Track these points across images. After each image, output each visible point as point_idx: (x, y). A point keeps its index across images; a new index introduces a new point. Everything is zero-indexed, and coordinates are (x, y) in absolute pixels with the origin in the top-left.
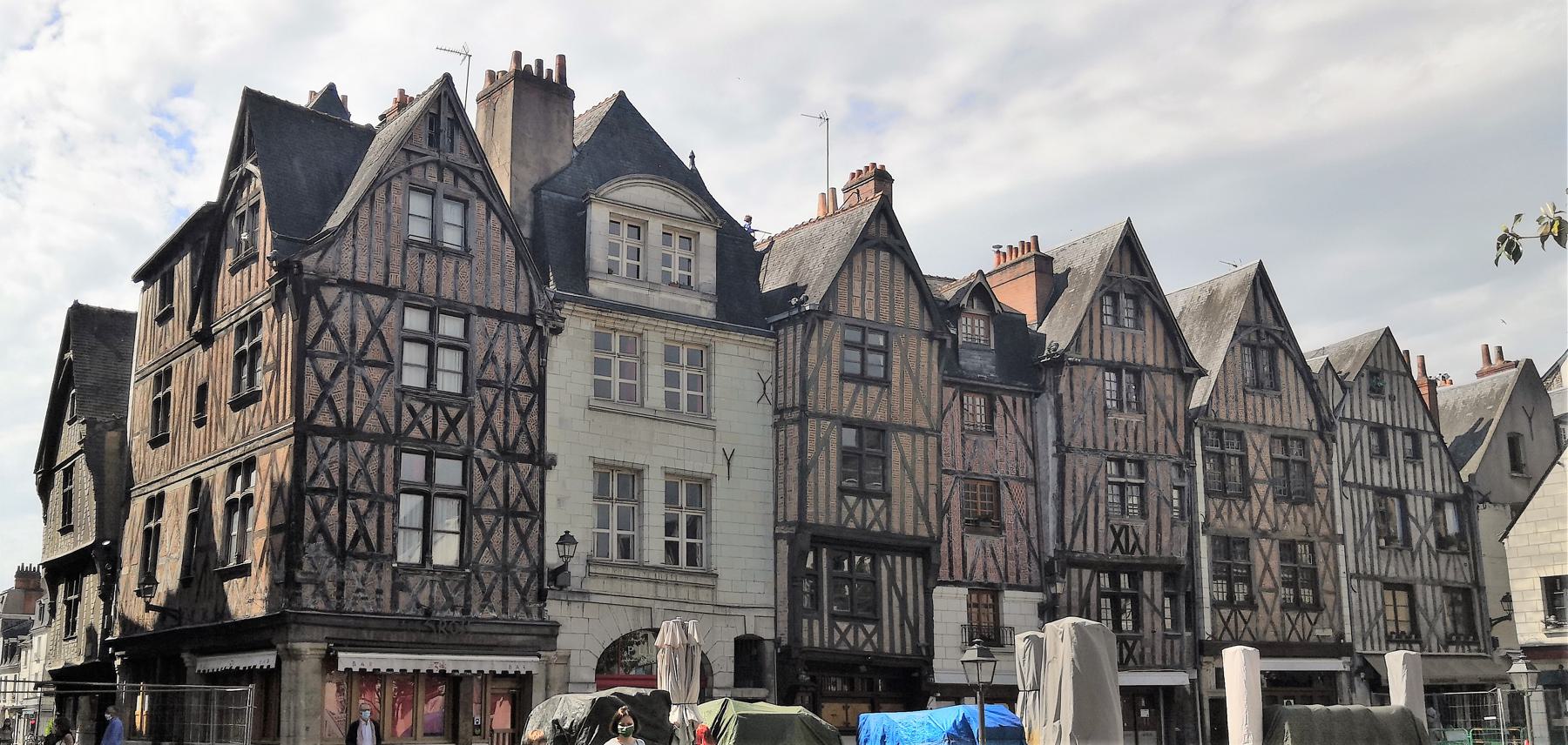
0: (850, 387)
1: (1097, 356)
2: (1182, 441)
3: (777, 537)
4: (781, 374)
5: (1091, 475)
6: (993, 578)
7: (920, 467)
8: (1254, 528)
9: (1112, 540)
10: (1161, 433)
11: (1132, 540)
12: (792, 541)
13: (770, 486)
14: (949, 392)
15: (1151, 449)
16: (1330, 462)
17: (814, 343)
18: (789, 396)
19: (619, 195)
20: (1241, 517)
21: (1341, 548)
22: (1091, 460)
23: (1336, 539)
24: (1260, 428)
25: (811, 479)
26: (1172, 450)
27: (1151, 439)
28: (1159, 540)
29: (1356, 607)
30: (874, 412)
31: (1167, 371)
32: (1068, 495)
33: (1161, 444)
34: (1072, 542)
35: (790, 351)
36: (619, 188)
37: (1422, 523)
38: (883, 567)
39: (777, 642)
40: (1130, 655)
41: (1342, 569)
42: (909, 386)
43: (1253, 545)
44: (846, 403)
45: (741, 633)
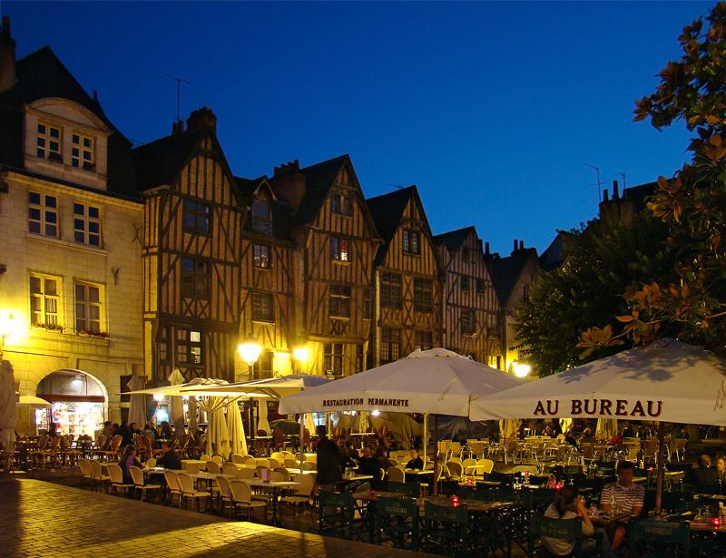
0: (188, 236)
1: (327, 229)
2: (369, 277)
4: (147, 225)
5: (322, 292)
8: (404, 324)
10: (359, 273)
13: (140, 291)
14: (246, 243)
15: (354, 281)
17: (167, 208)
19: (45, 109)
20: (397, 319)
21: (444, 335)
22: (323, 285)
24: (410, 273)
25: (164, 289)
26: (365, 282)
27: (354, 275)
30: (202, 251)
31: (363, 239)
33: (359, 277)
35: (153, 212)
36: (44, 105)
37: (482, 324)
42: (223, 237)
43: (403, 332)
44: (186, 245)
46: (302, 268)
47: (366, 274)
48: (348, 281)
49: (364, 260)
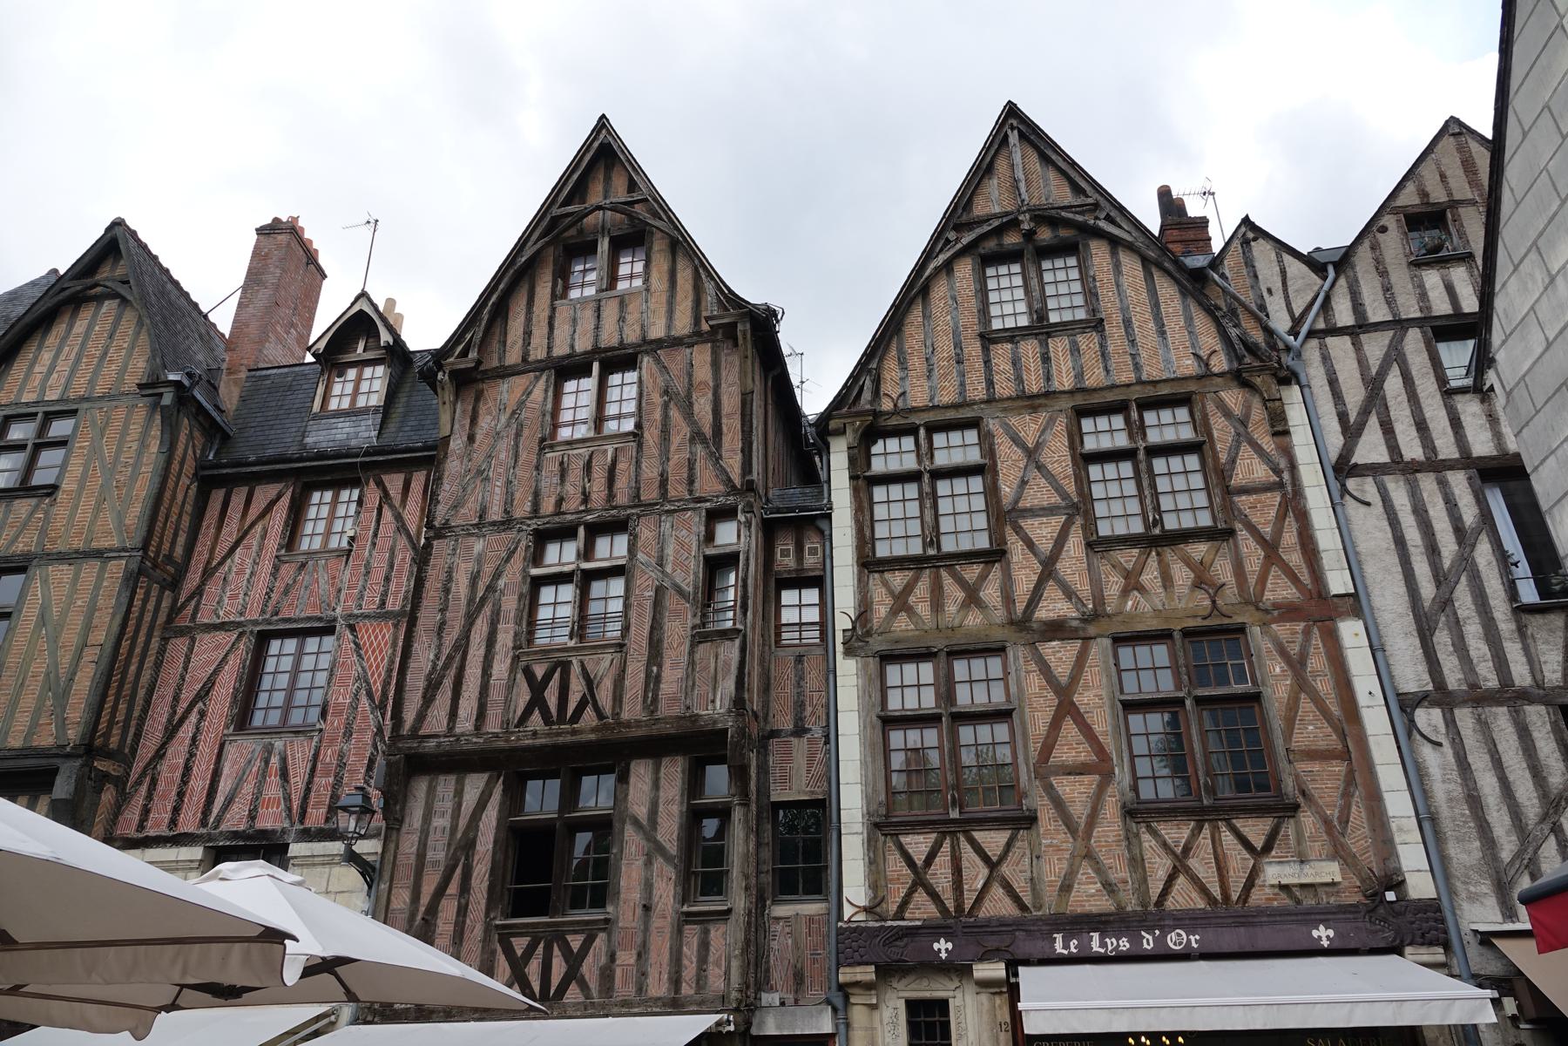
5: (488, 569)
6: (270, 819)
7: (76, 622)
8: (1022, 624)
9: (523, 695)
10: (678, 457)
11: (577, 689)
16: (1281, 431)
20: (973, 598)
23: (1321, 610)
24: (1030, 402)
28: (653, 681)
29: (1445, 786)
32: (428, 616)
34: (421, 717)
40: (572, 975)
41: (1365, 684)
47: (716, 458)
48: (622, 498)
49: (703, 406)
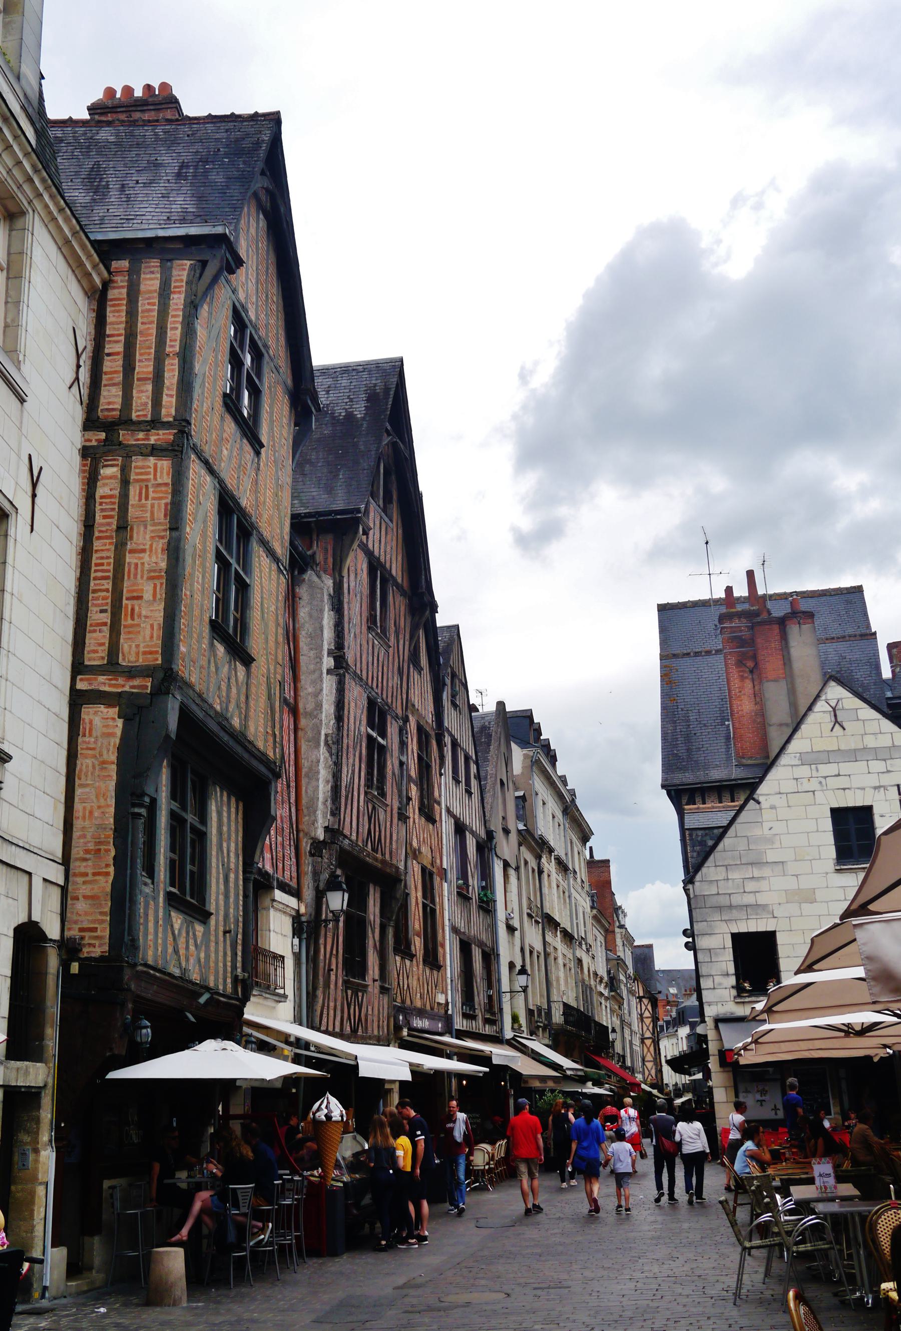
3: (78, 700)
12: (135, 711)
18: (142, 396)
21: (445, 885)
38: (214, 808)
39: (69, 948)
45: (22, 918)
46: (328, 634)
